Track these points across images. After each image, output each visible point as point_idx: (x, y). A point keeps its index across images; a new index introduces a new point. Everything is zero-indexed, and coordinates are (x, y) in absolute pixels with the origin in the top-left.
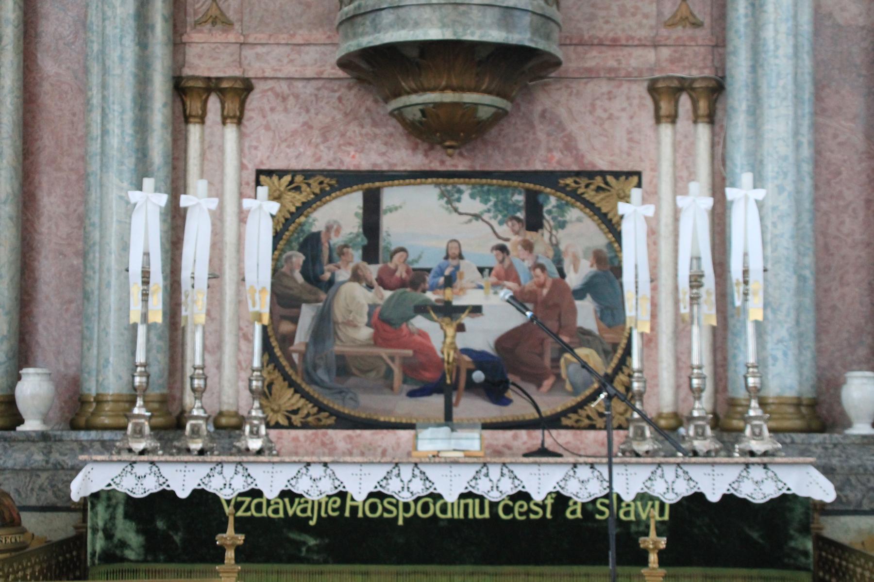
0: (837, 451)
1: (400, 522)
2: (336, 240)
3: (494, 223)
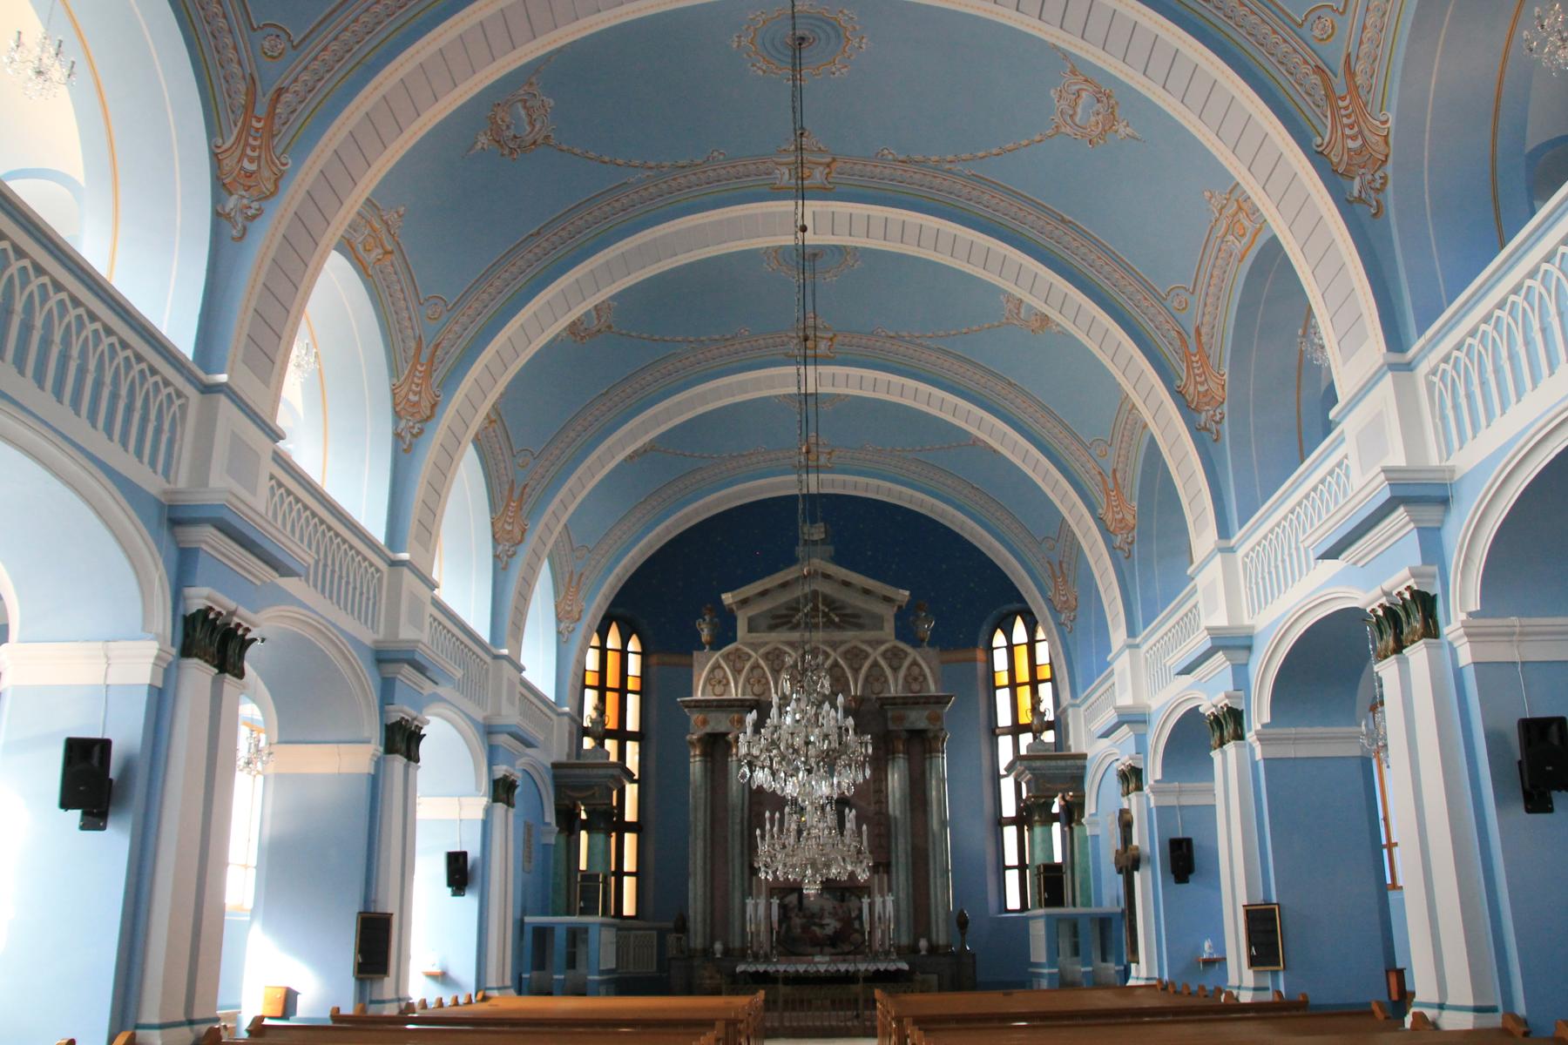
2: (791, 906)
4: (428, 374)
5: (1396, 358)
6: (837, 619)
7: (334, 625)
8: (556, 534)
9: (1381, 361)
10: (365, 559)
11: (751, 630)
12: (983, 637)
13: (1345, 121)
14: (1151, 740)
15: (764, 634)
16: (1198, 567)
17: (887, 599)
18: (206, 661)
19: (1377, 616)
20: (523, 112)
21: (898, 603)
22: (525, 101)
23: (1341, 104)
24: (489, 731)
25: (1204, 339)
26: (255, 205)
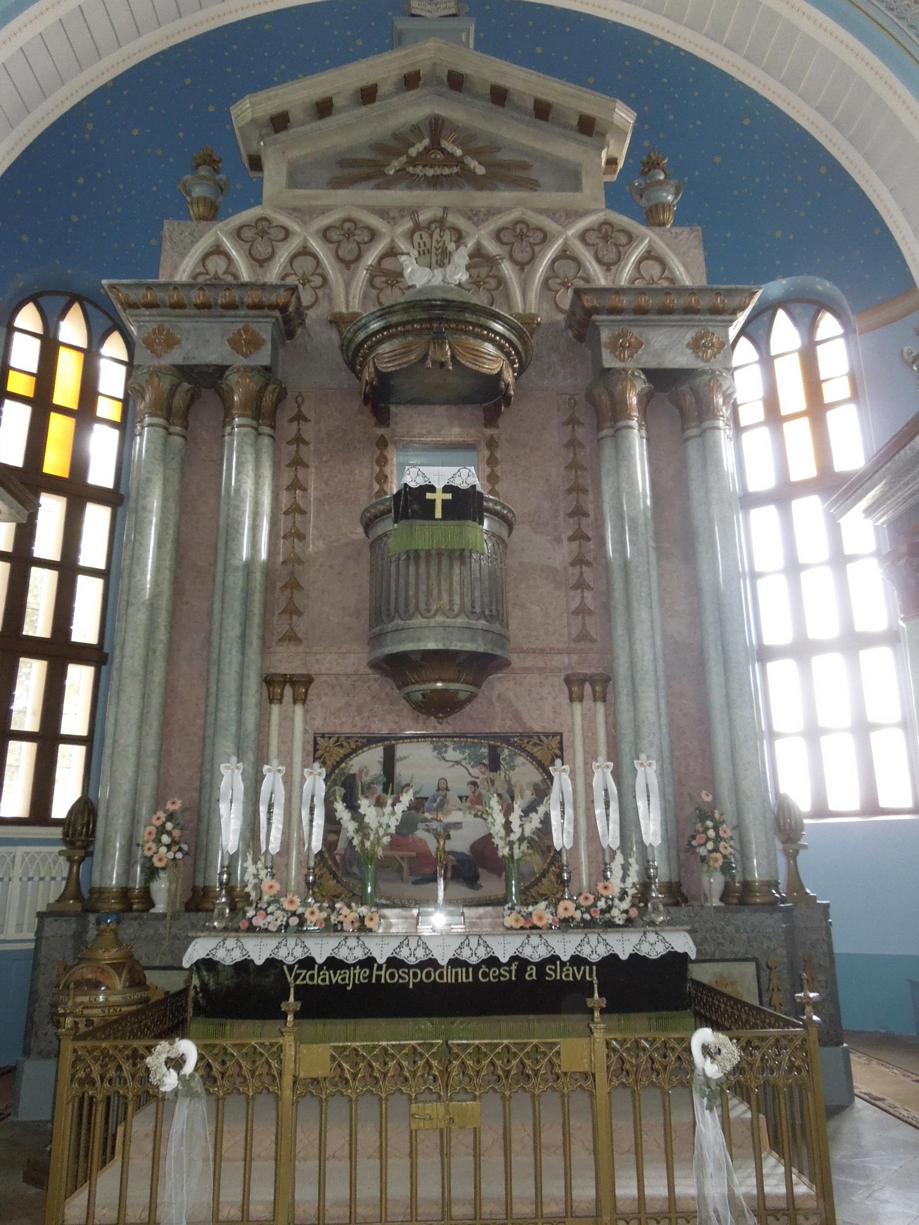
0: (697, 918)
1: (411, 986)
2: (366, 779)
3: (469, 767)
6: (480, 170)
15: (319, 192)
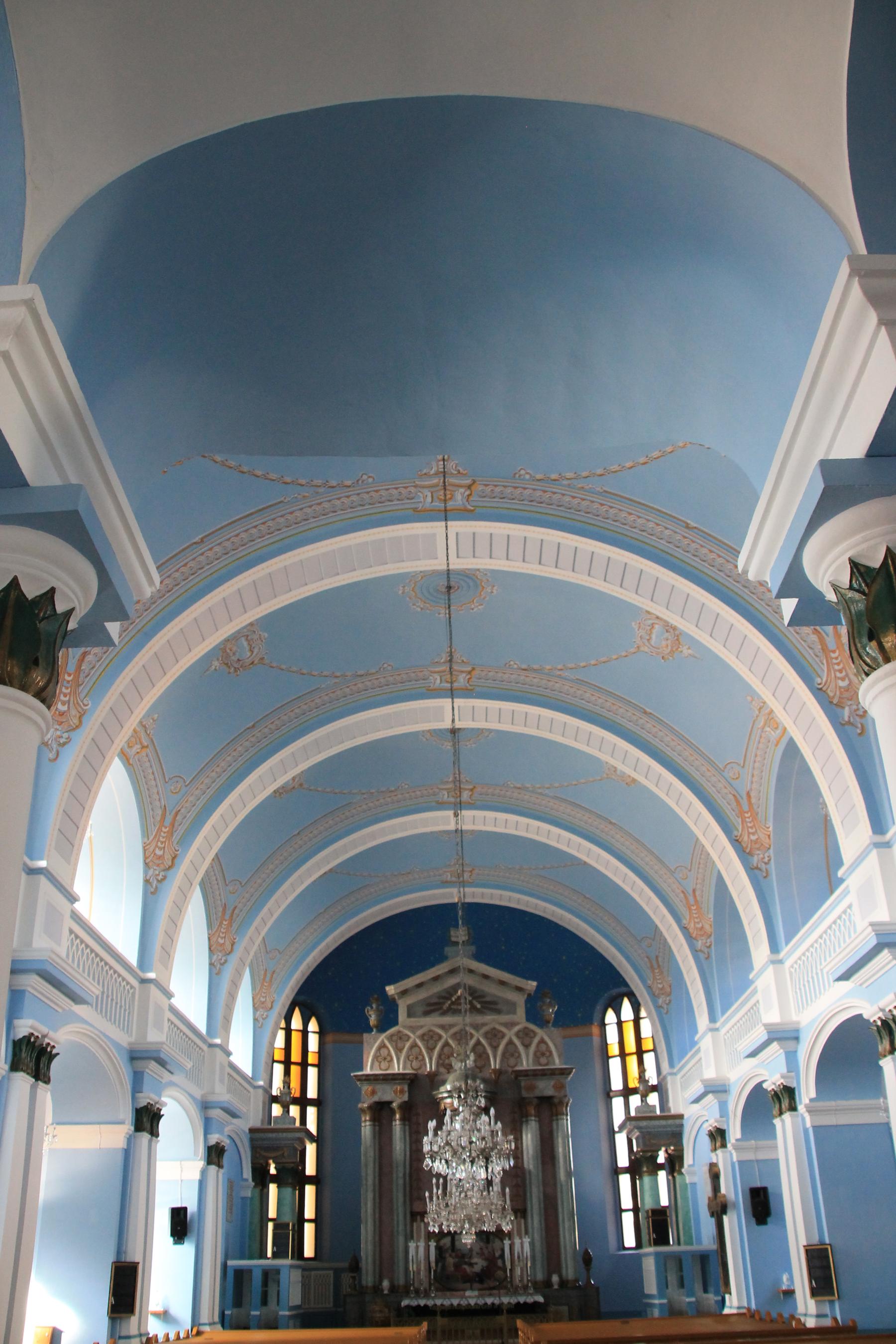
4: (171, 833)
5: (878, 839)
6: (479, 1006)
7: (105, 1035)
8: (257, 944)
9: (868, 842)
10: (124, 979)
11: (410, 1015)
12: (597, 1016)
13: (836, 667)
14: (731, 1106)
16: (756, 974)
17: (519, 989)
18: (28, 1074)
19: (877, 1026)
20: (245, 644)
21: (528, 992)
22: (248, 636)
23: (833, 655)
24: (205, 1106)
25: (753, 801)
26: (66, 735)
